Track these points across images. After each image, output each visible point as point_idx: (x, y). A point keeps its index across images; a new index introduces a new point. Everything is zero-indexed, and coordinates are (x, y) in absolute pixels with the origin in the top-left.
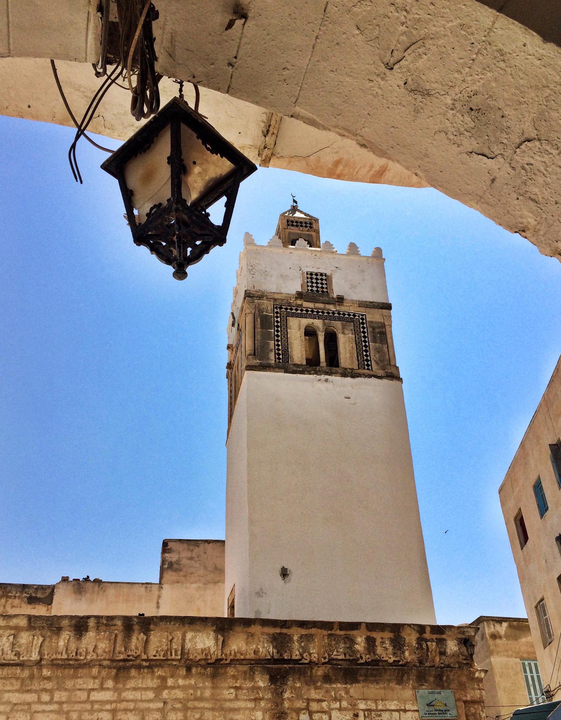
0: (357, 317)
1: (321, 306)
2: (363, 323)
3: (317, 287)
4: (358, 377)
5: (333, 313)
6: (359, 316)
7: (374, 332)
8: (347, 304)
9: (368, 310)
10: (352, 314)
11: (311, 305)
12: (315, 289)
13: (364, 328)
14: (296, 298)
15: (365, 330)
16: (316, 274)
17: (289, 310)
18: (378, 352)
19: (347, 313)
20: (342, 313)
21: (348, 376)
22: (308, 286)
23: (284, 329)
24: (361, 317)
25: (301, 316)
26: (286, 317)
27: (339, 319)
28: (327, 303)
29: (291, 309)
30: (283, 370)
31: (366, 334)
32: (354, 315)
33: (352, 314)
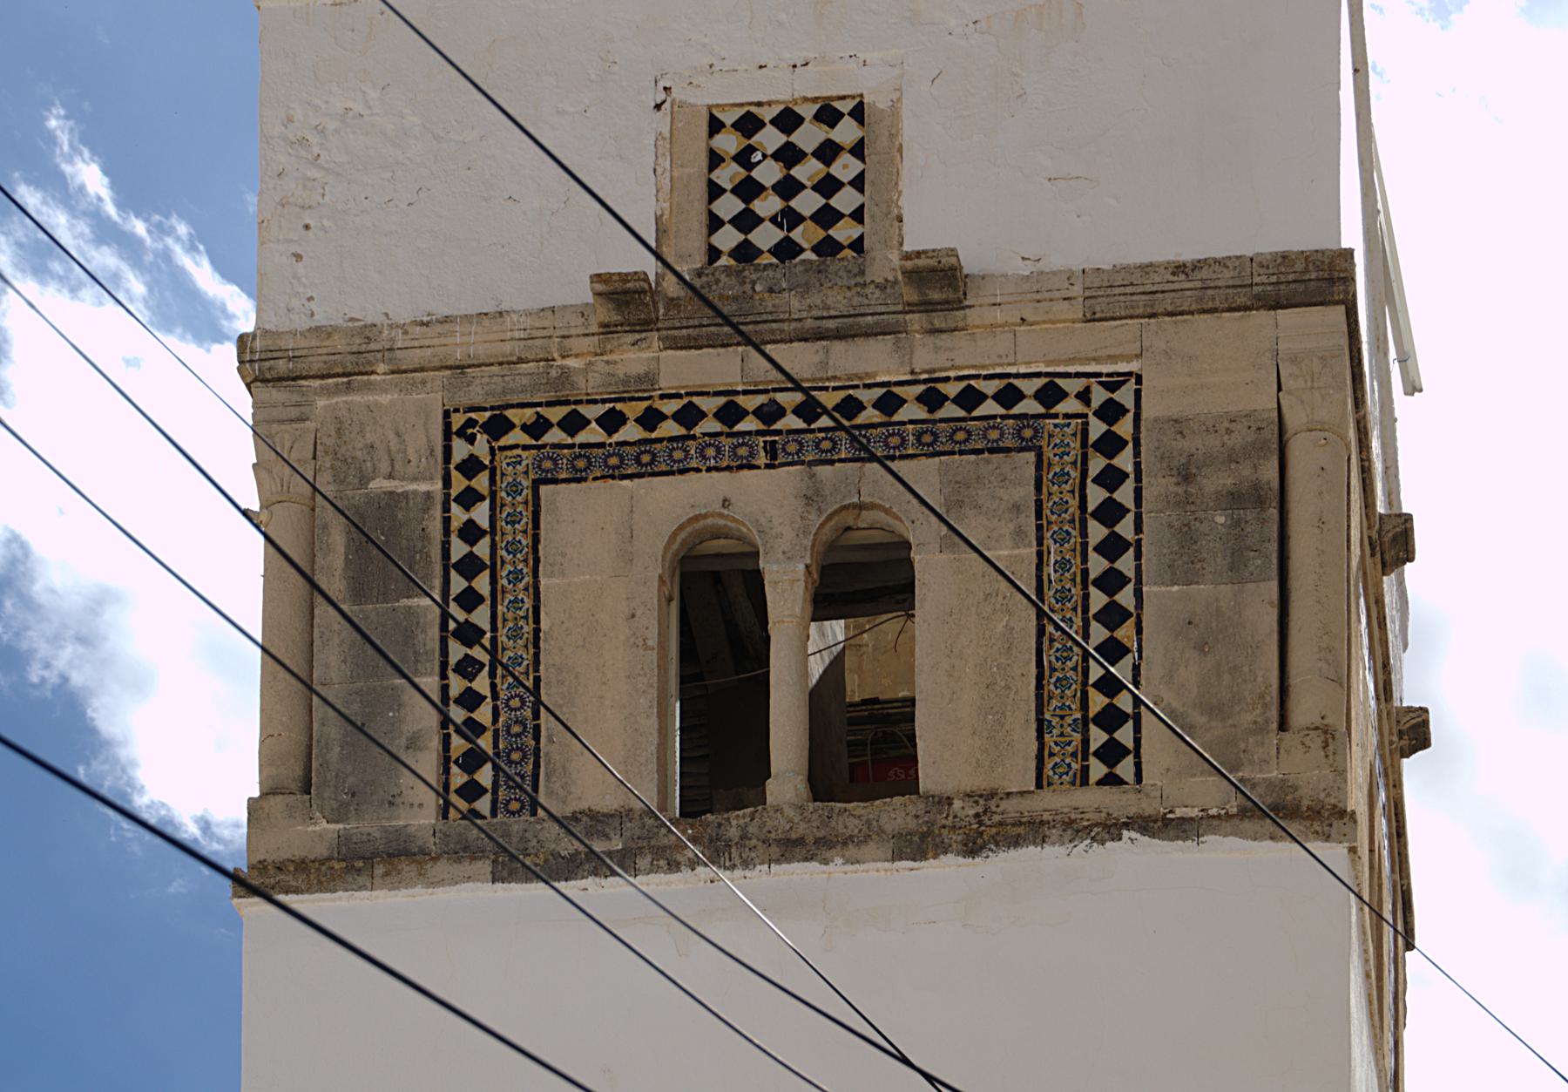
0: (1070, 405)
1: (800, 359)
2: (1110, 445)
3: (789, 218)
4: (1016, 842)
5: (889, 403)
6: (1084, 396)
7: (1186, 502)
8: (999, 316)
9: (1161, 334)
10: (1029, 387)
11: (719, 368)
12: (766, 237)
13: (1111, 479)
14: (607, 329)
15: (1125, 495)
16: (788, 120)
17: (555, 436)
18: (1201, 647)
19: (990, 388)
20: (952, 389)
21: (942, 849)
22: (715, 223)
23: (516, 576)
24: (1099, 396)
25: (644, 463)
26: (536, 484)
27: (930, 444)
28: (839, 335)
29: (573, 423)
30: (485, 867)
31: (1125, 528)
32: (1050, 394)
33: (1029, 387)
